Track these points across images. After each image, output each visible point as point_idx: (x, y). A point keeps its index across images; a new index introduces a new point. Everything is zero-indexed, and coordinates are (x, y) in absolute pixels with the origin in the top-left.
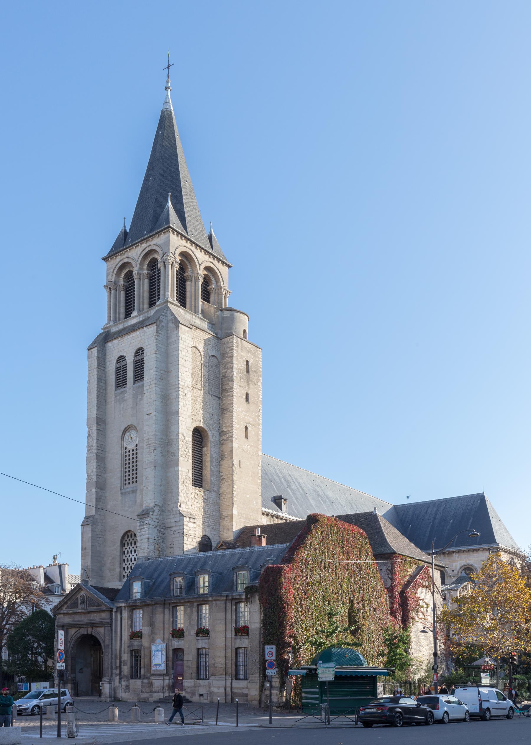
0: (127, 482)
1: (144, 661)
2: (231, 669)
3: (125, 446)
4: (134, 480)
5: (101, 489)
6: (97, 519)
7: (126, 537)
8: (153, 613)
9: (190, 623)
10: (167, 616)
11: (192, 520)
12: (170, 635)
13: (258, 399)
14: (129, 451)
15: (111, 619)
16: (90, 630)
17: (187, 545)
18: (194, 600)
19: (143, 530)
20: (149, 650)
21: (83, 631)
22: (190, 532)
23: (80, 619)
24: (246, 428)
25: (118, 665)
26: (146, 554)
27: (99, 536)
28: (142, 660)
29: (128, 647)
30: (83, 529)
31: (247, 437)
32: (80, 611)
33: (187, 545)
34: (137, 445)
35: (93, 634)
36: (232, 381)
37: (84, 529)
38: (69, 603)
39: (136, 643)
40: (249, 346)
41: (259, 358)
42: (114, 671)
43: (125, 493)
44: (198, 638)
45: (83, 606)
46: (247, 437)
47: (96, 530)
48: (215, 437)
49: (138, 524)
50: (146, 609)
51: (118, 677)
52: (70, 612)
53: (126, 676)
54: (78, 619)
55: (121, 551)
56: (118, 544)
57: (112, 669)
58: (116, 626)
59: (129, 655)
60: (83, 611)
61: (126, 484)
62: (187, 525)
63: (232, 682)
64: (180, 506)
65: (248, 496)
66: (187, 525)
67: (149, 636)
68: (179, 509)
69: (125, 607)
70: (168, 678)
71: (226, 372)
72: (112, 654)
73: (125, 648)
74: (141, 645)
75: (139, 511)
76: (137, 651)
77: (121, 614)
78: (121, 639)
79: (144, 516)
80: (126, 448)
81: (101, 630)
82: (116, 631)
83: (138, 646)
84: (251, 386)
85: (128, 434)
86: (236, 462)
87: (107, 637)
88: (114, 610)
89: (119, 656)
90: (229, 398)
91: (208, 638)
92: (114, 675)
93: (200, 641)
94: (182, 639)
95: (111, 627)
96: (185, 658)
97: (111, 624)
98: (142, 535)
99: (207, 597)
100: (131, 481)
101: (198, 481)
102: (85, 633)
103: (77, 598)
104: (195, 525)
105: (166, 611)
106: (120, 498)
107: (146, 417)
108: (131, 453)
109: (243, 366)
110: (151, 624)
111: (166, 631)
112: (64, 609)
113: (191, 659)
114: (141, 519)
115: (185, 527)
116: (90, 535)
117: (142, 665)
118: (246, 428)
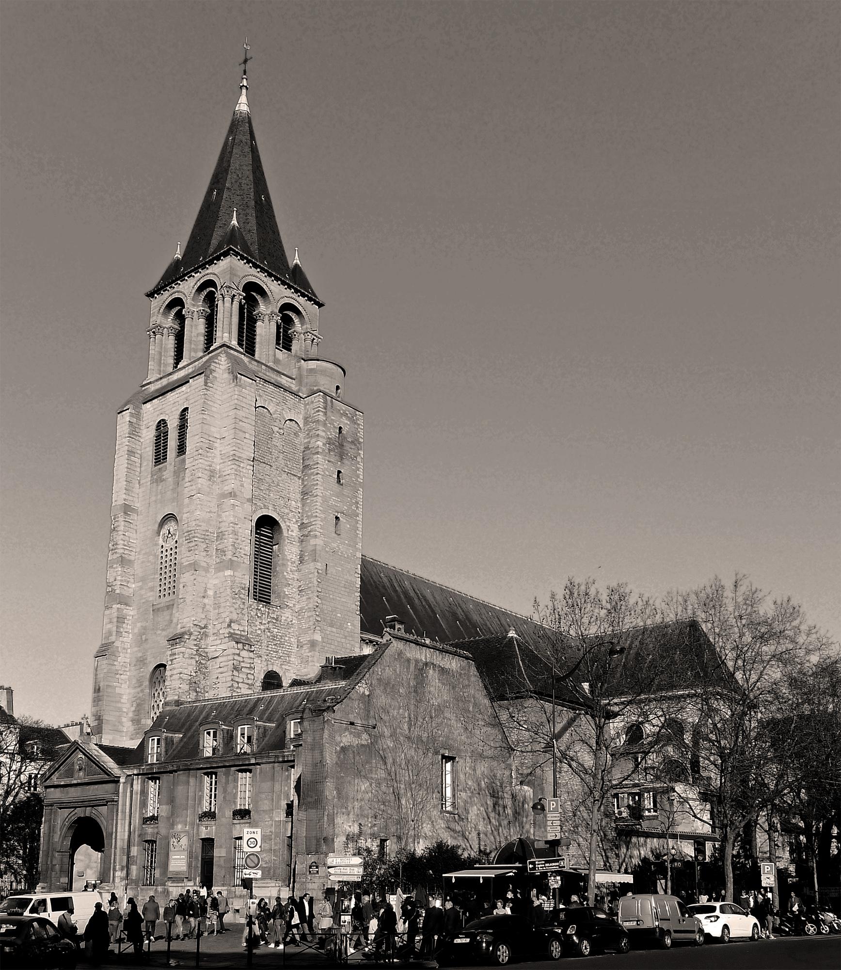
1: (158, 858)
2: (282, 870)
5: (126, 604)
8: (175, 784)
10: (191, 789)
12: (197, 817)
13: (357, 480)
15: (118, 794)
17: (238, 683)
21: (80, 812)
22: (243, 664)
23: (74, 795)
24: (337, 518)
25: (124, 863)
26: (176, 698)
27: (120, 672)
29: (139, 836)
32: (75, 782)
33: (238, 683)
35: (93, 816)
39: (150, 830)
40: (344, 407)
41: (359, 425)
42: (118, 874)
43: (158, 609)
44: (235, 821)
45: (81, 774)
48: (292, 531)
49: (170, 653)
50: (164, 777)
51: (123, 883)
53: (136, 882)
54: (73, 794)
55: (150, 694)
56: (147, 683)
57: (114, 870)
58: (124, 804)
60: (79, 781)
63: (279, 891)
64: (229, 626)
65: (339, 615)
66: (239, 655)
67: (168, 818)
69: (137, 775)
71: (309, 442)
72: (115, 848)
73: (136, 839)
75: (171, 632)
76: (152, 842)
77: (132, 786)
78: (130, 822)
81: (104, 809)
82: (124, 812)
84: (346, 461)
85: (166, 527)
88: (122, 780)
91: (248, 821)
92: (117, 880)
93: (238, 826)
94: (213, 823)
95: (118, 805)
96: (217, 853)
98: (174, 669)
99: (249, 759)
101: (262, 592)
104: (251, 655)
105: (192, 781)
106: (152, 617)
107: (187, 501)
109: (334, 434)
110: (171, 801)
112: (54, 777)
114: (172, 645)
118: (337, 518)
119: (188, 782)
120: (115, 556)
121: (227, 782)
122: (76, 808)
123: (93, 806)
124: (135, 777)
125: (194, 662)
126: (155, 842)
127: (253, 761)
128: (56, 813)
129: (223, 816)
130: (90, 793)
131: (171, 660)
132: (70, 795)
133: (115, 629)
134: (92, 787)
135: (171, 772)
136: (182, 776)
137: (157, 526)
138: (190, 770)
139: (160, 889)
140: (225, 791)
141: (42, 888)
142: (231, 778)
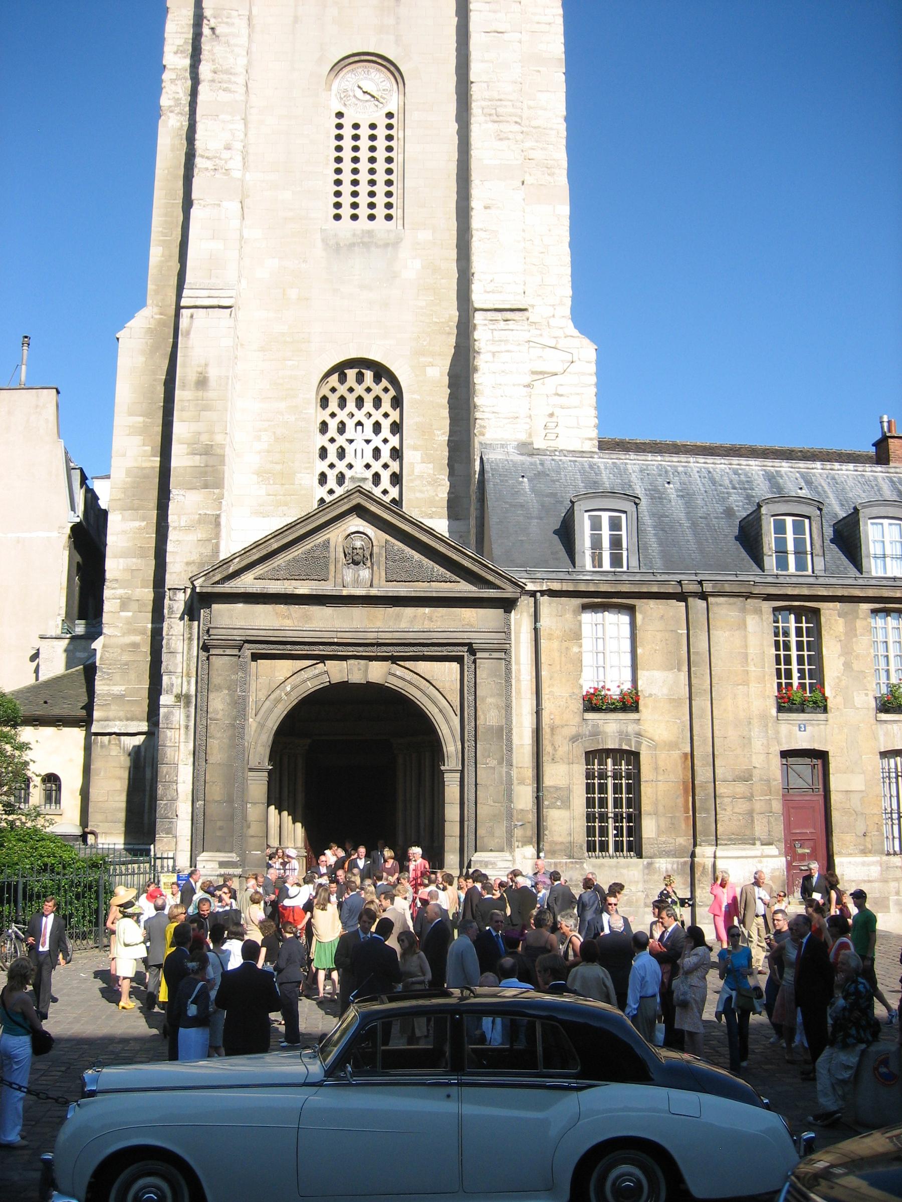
0: (346, 211)
4: (380, 211)
7: (336, 376)
9: (847, 665)
14: (356, 126)
15: (508, 633)
16: (377, 672)
18: (870, 593)
20: (676, 754)
21: (338, 672)
28: (646, 790)
29: (574, 739)
38: (281, 560)
44: (884, 716)
45: (365, 573)
52: (303, 588)
59: (580, 769)
60: (374, 592)
61: (337, 217)
67: (674, 701)
69: (552, 593)
70: (773, 850)
74: (639, 734)
77: (536, 618)
81: (446, 674)
83: (623, 736)
87: (490, 700)
89: (529, 773)
94: (822, 716)
95: (508, 663)
97: (506, 651)
100: (363, 211)
102: (356, 677)
103: (326, 544)
108: (364, 132)
111: (754, 688)
113: (863, 788)
117: (646, 806)
119: (743, 626)
120: (224, 97)
121: (851, 632)
122: (322, 659)
123: (394, 659)
124: (544, 600)
126: (637, 755)
128: (243, 668)
129: (848, 702)
130: (403, 625)
131: (494, 354)
132: (316, 624)
134: (409, 611)
135: (682, 597)
136: (723, 609)
138: (748, 596)
139: (664, 864)
140: (847, 651)
141: (222, 864)
142: (859, 624)
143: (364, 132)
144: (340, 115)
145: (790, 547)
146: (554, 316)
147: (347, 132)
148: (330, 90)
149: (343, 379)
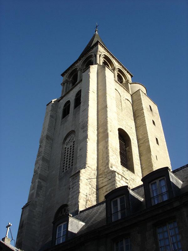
0: (64, 170)
3: (65, 146)
5: (43, 180)
6: (36, 202)
11: (124, 179)
14: (68, 148)
19: (75, 187)
30: (23, 211)
31: (158, 143)
34: (74, 142)
36: (143, 109)
37: (24, 211)
46: (158, 143)
47: (34, 211)
48: (135, 141)
61: (63, 171)
62: (119, 181)
66: (119, 181)
68: (111, 169)
79: (76, 175)
80: (66, 148)
86: (152, 153)
90: (142, 119)
100: (67, 168)
106: (58, 182)
108: (69, 149)
115: (118, 182)
116: (27, 213)
118: (157, 139)
125: (88, 188)
127: (176, 204)
131: (73, 188)
133: (36, 192)
137: (63, 140)
143: (69, 149)
144: (66, 148)
145: (119, 209)
146: (105, 169)
147: (67, 150)
148: (64, 144)
149: (62, 213)
